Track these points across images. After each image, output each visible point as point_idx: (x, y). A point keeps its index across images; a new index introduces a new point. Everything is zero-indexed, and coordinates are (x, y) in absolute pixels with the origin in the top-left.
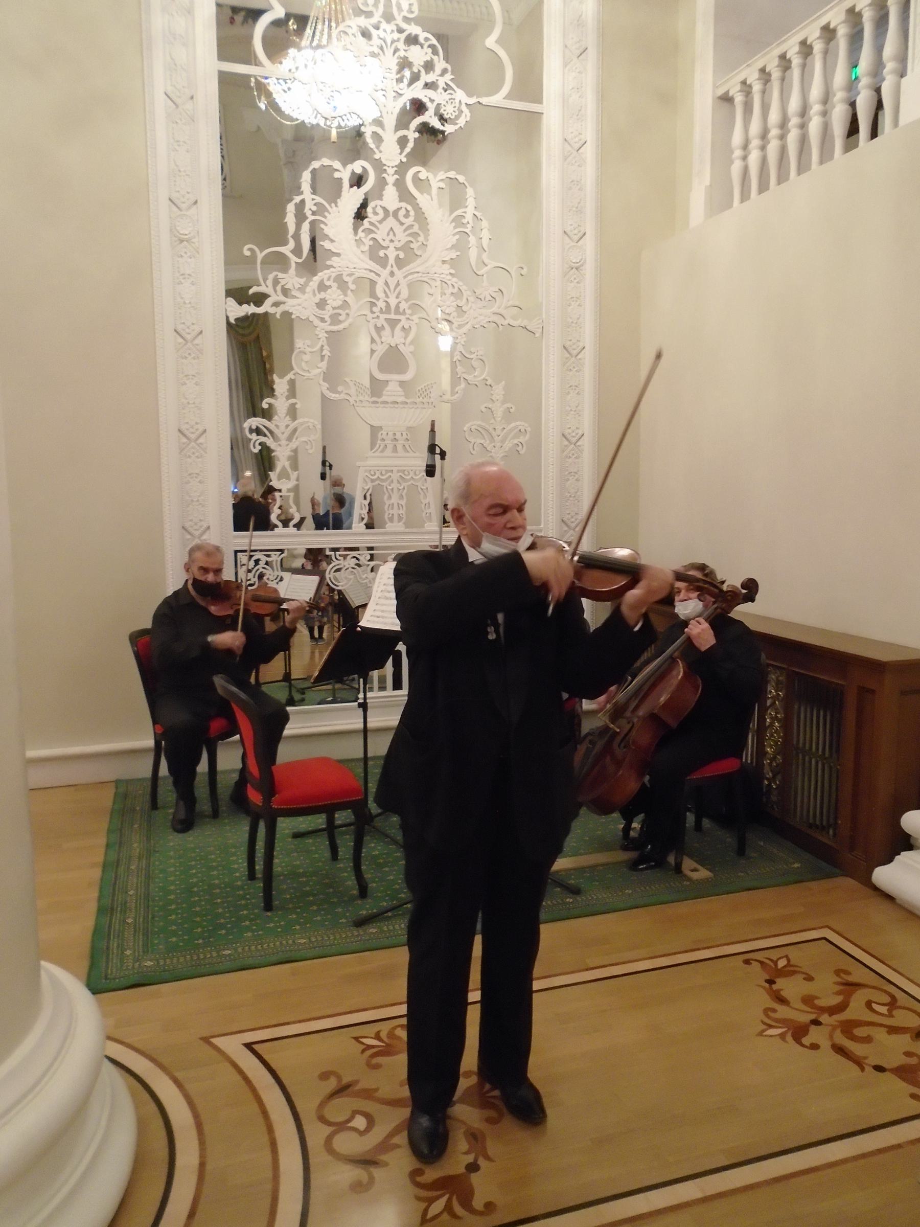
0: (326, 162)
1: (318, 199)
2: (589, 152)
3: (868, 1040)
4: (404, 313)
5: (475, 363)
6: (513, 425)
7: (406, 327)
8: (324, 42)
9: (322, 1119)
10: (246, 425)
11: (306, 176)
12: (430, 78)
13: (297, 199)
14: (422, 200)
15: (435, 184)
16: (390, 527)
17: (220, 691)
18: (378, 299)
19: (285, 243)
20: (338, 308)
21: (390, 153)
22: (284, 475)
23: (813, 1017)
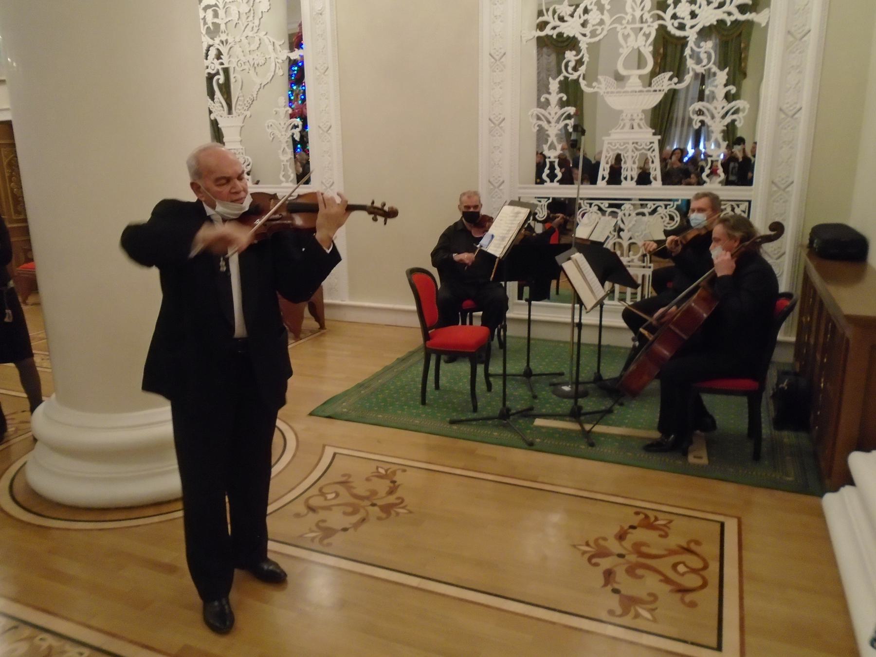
3: (641, 577)
4: (646, 22)
5: (703, 56)
6: (733, 103)
7: (647, 32)
9: (320, 490)
18: (626, 14)
20: (597, 24)
22: (552, 147)
23: (623, 552)
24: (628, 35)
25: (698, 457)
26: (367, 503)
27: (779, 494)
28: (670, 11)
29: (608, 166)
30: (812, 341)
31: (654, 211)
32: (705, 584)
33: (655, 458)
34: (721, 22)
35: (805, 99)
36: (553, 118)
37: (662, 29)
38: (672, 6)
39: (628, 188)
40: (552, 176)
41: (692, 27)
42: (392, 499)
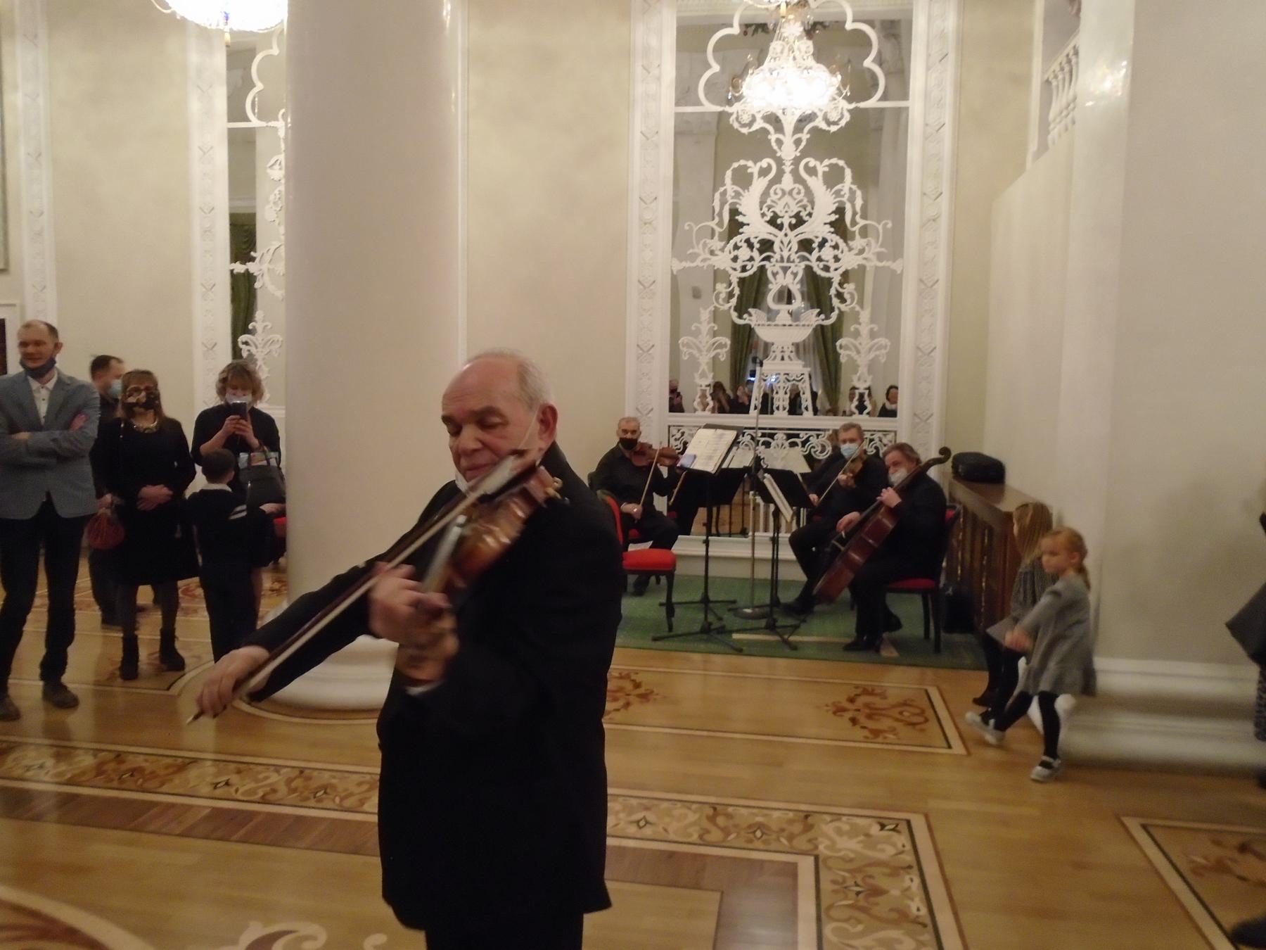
0: (742, 162)
2: (947, 132)
5: (847, 296)
11: (729, 173)
13: (722, 189)
14: (811, 181)
21: (788, 152)
22: (703, 375)
25: (888, 652)
26: (618, 694)
27: (964, 672)
28: (815, 254)
30: (968, 556)
31: (807, 440)
32: (927, 720)
33: (853, 655)
35: (938, 340)
37: (809, 269)
39: (781, 418)
42: (641, 690)
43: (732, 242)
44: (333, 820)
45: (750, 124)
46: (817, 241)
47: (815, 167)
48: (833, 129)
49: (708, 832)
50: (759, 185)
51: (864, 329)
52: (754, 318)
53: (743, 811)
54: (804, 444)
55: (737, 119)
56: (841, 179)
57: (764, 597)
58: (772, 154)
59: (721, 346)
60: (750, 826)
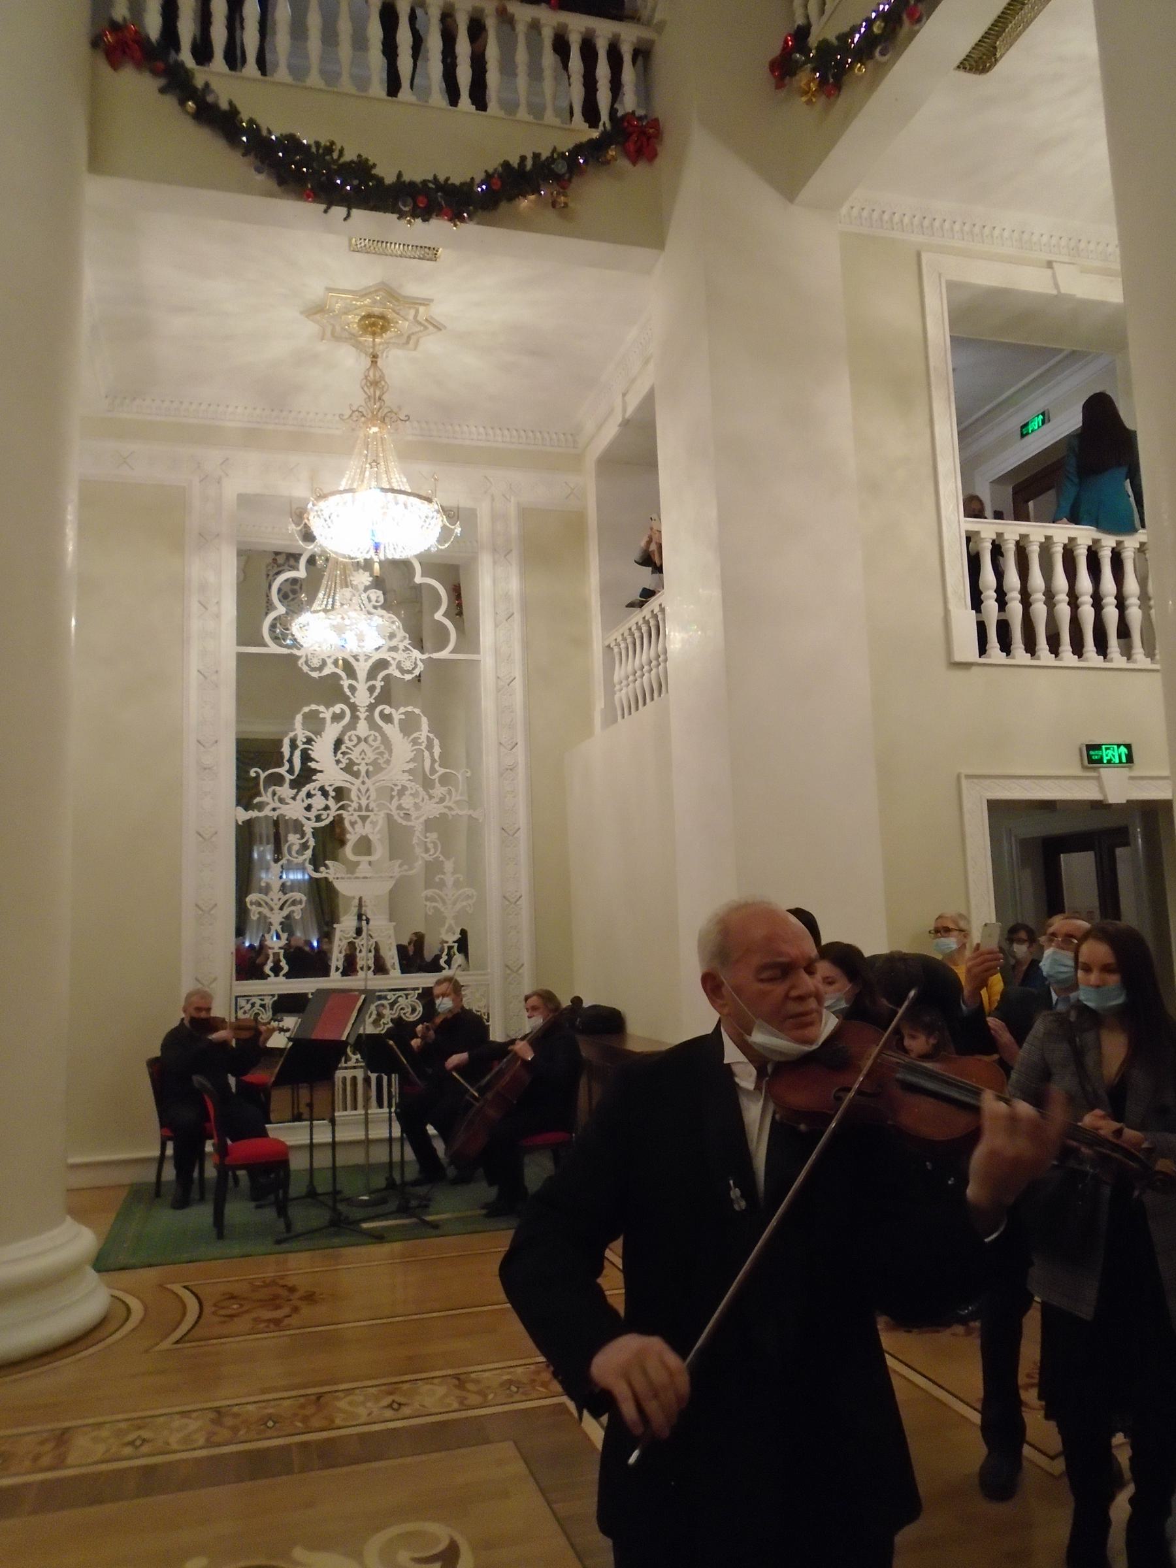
0: (314, 707)
1: (309, 734)
2: (518, 685)
5: (430, 846)
8: (329, 607)
9: (215, 1305)
10: (248, 899)
11: (299, 718)
12: (393, 643)
13: (291, 734)
14: (387, 728)
15: (397, 716)
16: (361, 974)
17: (196, 1085)
19: (281, 765)
21: (362, 698)
24: (356, 822)
28: (395, 802)
29: (342, 956)
31: (395, 1002)
34: (443, 816)
35: (524, 887)
36: (276, 905)
38: (396, 798)
40: (276, 970)
41: (417, 818)
43: (305, 790)
44: (43, 1482)
45: (320, 669)
46: (396, 788)
47: (390, 714)
48: (408, 677)
49: (466, 1398)
50: (331, 732)
51: (449, 879)
52: (332, 871)
53: (487, 1374)
54: (392, 1005)
55: (306, 662)
56: (419, 729)
57: (379, 1182)
58: (345, 700)
59: (294, 903)
60: (502, 1384)
